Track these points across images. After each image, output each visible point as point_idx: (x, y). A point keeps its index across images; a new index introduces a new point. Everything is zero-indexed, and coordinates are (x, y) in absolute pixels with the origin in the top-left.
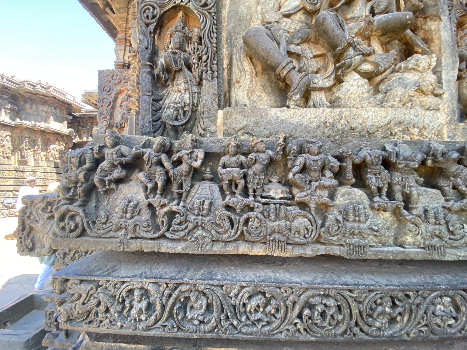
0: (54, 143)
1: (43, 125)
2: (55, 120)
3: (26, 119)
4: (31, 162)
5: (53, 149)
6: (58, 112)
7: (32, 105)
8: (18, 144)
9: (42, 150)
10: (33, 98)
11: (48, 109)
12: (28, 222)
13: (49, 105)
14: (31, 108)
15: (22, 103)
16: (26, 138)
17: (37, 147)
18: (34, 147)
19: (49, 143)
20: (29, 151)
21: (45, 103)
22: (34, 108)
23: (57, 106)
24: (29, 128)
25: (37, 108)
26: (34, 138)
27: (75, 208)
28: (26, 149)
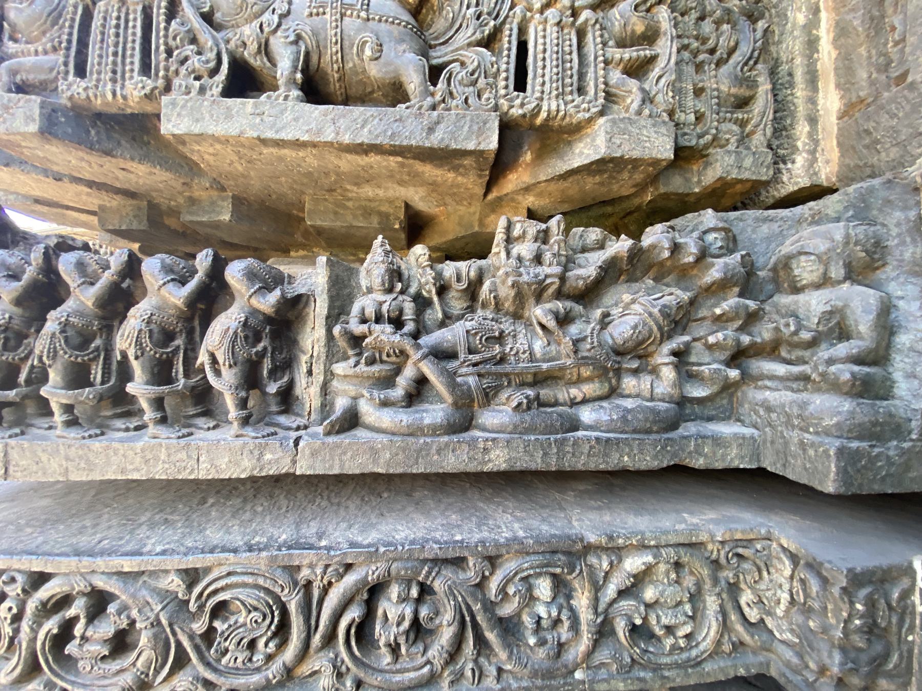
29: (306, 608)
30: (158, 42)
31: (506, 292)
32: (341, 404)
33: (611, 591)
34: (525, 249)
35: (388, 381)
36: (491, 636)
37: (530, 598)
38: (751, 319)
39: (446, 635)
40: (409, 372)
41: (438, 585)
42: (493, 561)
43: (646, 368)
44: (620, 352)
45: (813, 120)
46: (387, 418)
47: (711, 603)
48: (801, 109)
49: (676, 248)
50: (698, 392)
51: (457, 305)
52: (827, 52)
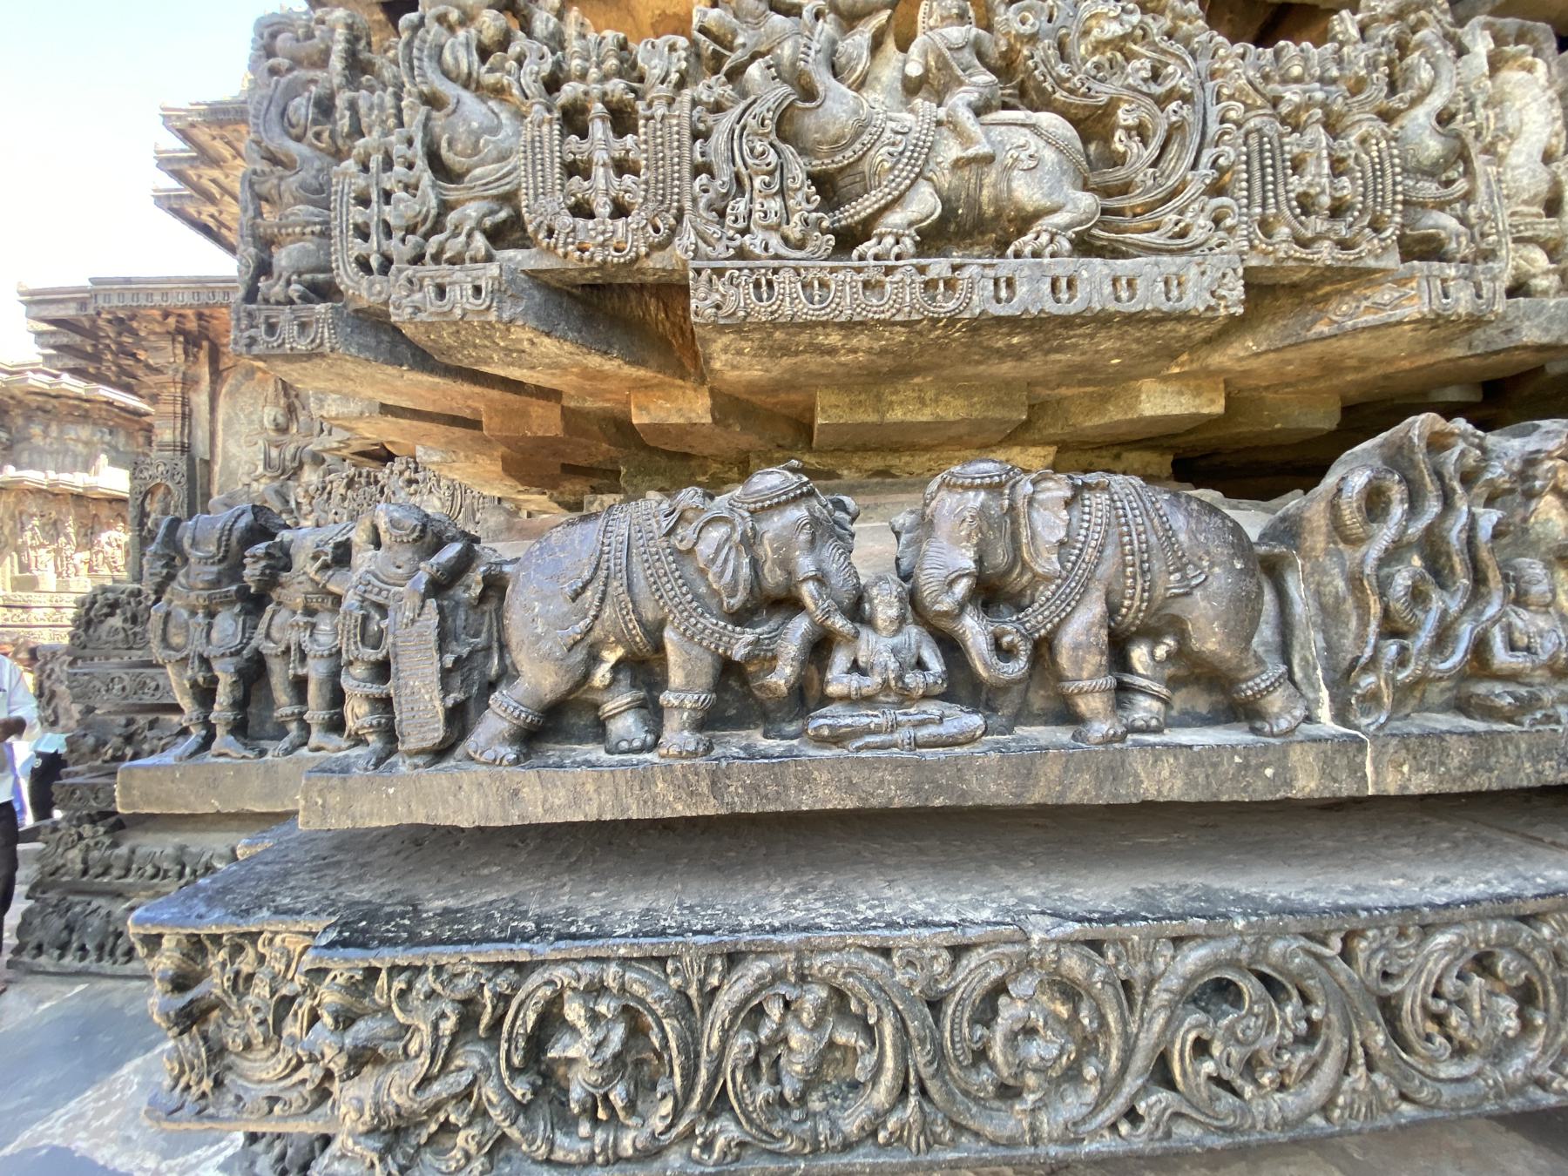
0: (109, 527)
1: (78, 480)
2: (113, 462)
3: (31, 466)
4: (48, 580)
5: (110, 544)
6: (121, 441)
7: (47, 426)
8: (12, 532)
9: (79, 548)
10: (49, 407)
11: (93, 434)
12: (47, 684)
13: (95, 424)
14: (46, 433)
15: (20, 421)
16: (32, 516)
17: (62, 540)
18: (54, 539)
19: (97, 528)
20: (42, 552)
21: (85, 417)
22: (54, 434)
23: (118, 425)
24: (40, 491)
25: (61, 432)
26: (54, 515)
27: (80, 632)
28: (32, 547)
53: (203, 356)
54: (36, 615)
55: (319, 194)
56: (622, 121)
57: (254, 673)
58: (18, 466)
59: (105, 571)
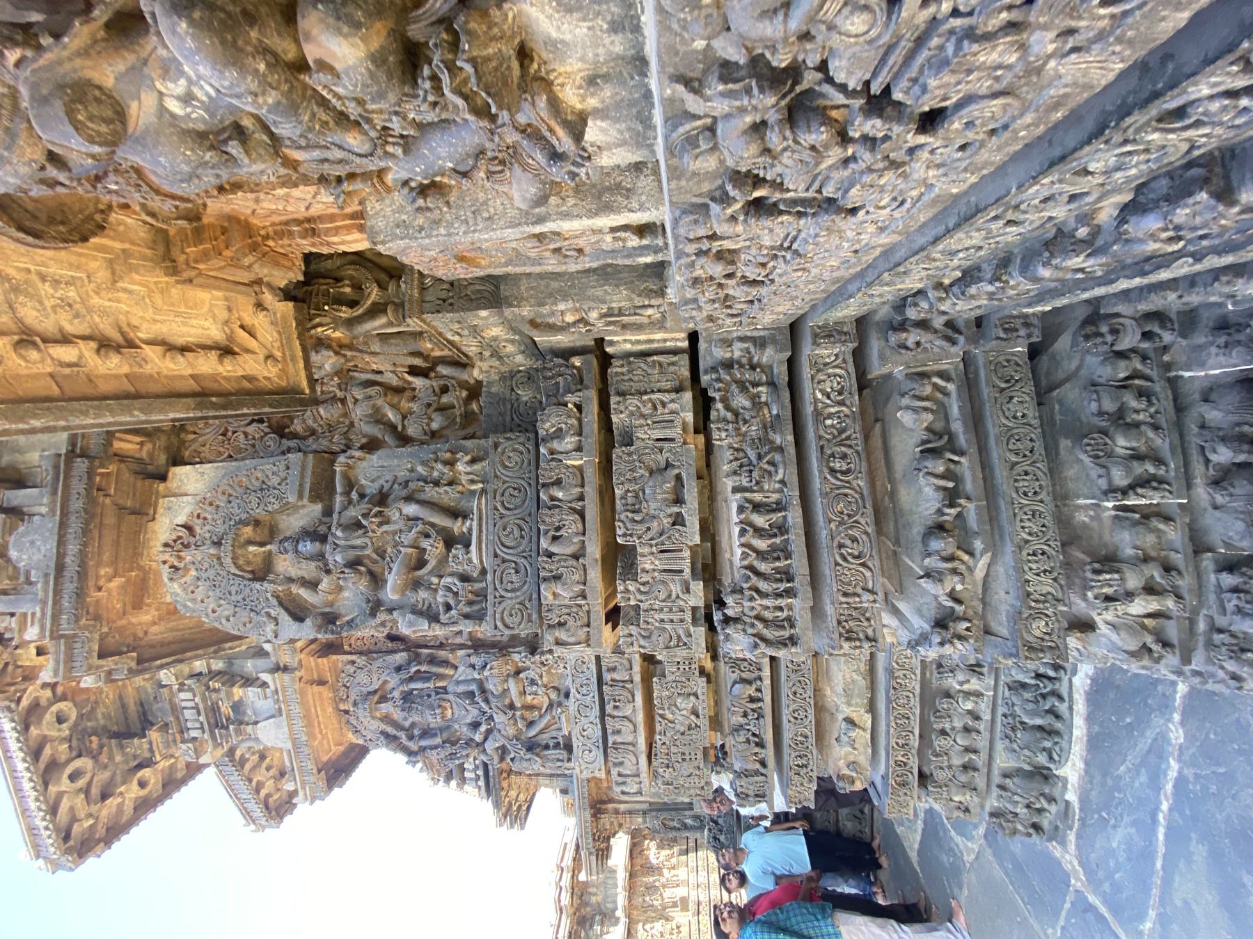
0: (647, 858)
3: (615, 902)
4: (681, 892)
14: (595, 894)
15: (588, 909)
17: (657, 884)
20: (665, 895)
29: (839, 488)
30: (671, 547)
31: (737, 439)
32: (777, 486)
33: (828, 401)
34: (724, 435)
35: (770, 473)
36: (844, 436)
37: (833, 426)
38: (741, 366)
39: (843, 449)
40: (766, 466)
41: (829, 452)
42: (820, 437)
43: (758, 395)
44: (754, 404)
45: (665, 341)
46: (781, 471)
47: (831, 371)
48: (661, 345)
49: (719, 390)
50: (764, 378)
51: (741, 454)
52: (643, 337)
53: (604, 807)
54: (703, 898)
55: (689, 788)
56: (683, 754)
57: (757, 796)
58: (616, 909)
59: (674, 860)
